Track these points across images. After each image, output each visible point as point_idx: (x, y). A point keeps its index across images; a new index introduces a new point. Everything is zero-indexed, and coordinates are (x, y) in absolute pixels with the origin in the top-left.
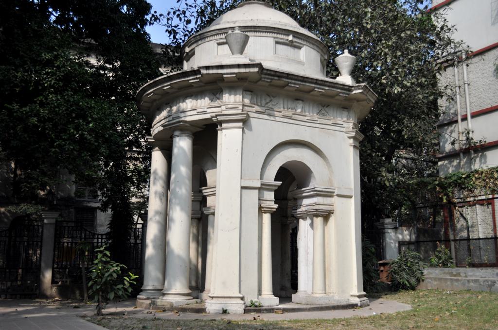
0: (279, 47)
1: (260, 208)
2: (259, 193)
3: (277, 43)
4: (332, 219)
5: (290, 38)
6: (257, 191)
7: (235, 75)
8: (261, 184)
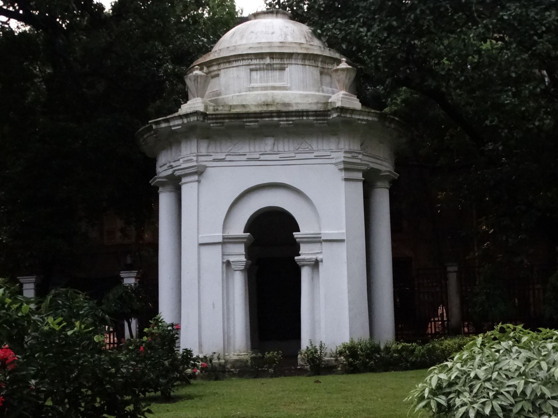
0: (254, 73)
1: (228, 264)
2: (222, 248)
3: (251, 70)
4: (321, 267)
5: (268, 61)
6: (220, 247)
7: (180, 127)
8: (224, 238)
